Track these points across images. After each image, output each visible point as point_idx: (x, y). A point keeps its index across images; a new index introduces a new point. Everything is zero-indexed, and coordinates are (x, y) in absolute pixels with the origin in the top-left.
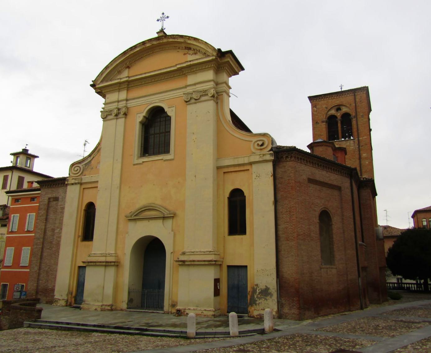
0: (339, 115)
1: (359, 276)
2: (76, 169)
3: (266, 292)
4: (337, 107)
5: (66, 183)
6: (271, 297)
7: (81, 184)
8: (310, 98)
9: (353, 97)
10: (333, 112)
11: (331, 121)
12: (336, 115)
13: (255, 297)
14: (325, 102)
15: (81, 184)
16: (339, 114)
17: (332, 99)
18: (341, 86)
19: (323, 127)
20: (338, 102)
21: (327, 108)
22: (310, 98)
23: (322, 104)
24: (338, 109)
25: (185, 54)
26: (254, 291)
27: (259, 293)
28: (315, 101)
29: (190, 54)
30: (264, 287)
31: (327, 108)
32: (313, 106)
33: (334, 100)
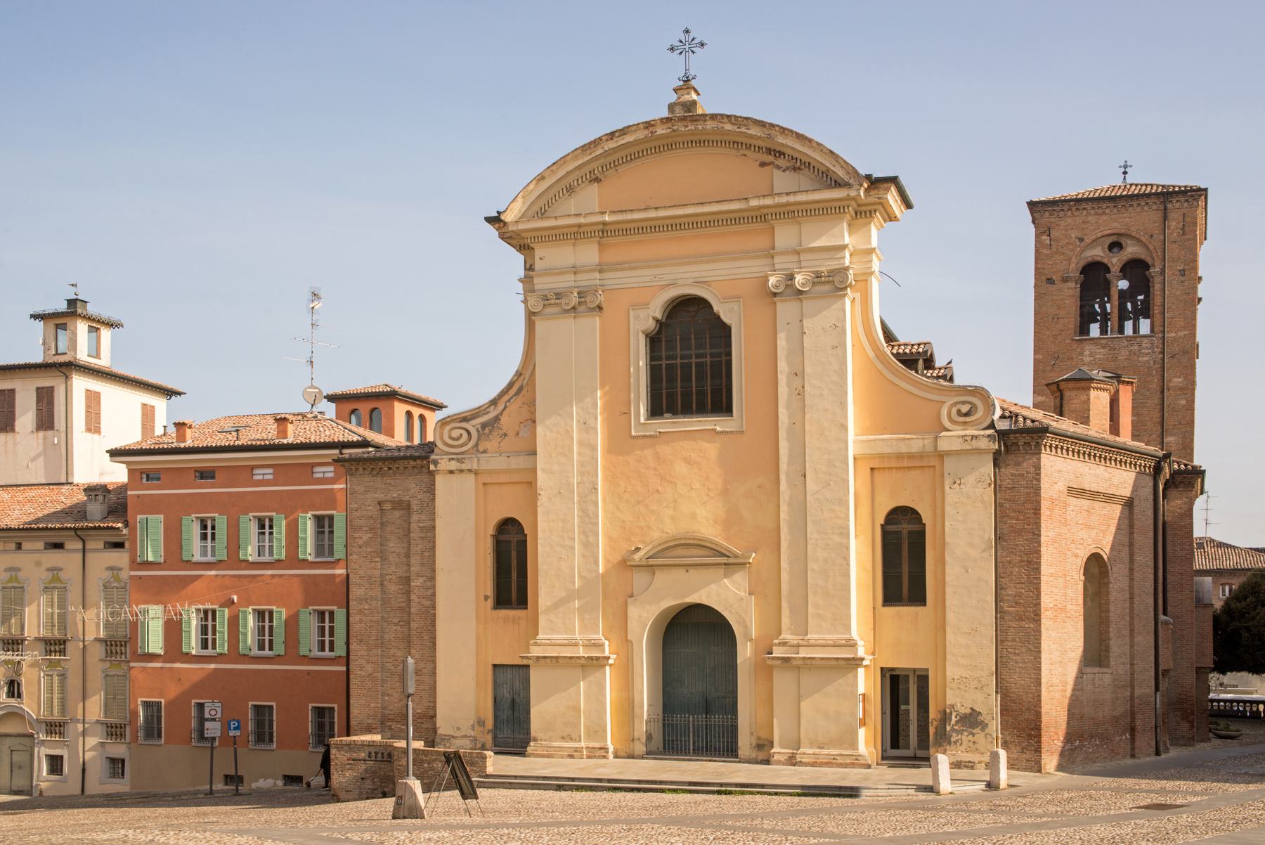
0: (1115, 262)
1: (1157, 689)
2: (455, 433)
3: (972, 720)
4: (1110, 240)
5: (432, 467)
6: (983, 730)
7: (476, 473)
8: (1031, 205)
9: (1160, 214)
10: (1098, 253)
11: (1094, 277)
12: (1105, 261)
13: (948, 728)
14: (1079, 220)
15: (476, 473)
16: (1115, 260)
17: (1097, 214)
18: (1125, 167)
19: (1069, 294)
20: (1115, 225)
21: (1081, 240)
22: (1031, 205)
23: (1068, 225)
24: (1116, 246)
25: (763, 165)
26: (945, 718)
27: (957, 722)
28: (1047, 214)
29: (778, 167)
30: (968, 711)
31: (1081, 240)
32: (1043, 231)
33: (1105, 218)
